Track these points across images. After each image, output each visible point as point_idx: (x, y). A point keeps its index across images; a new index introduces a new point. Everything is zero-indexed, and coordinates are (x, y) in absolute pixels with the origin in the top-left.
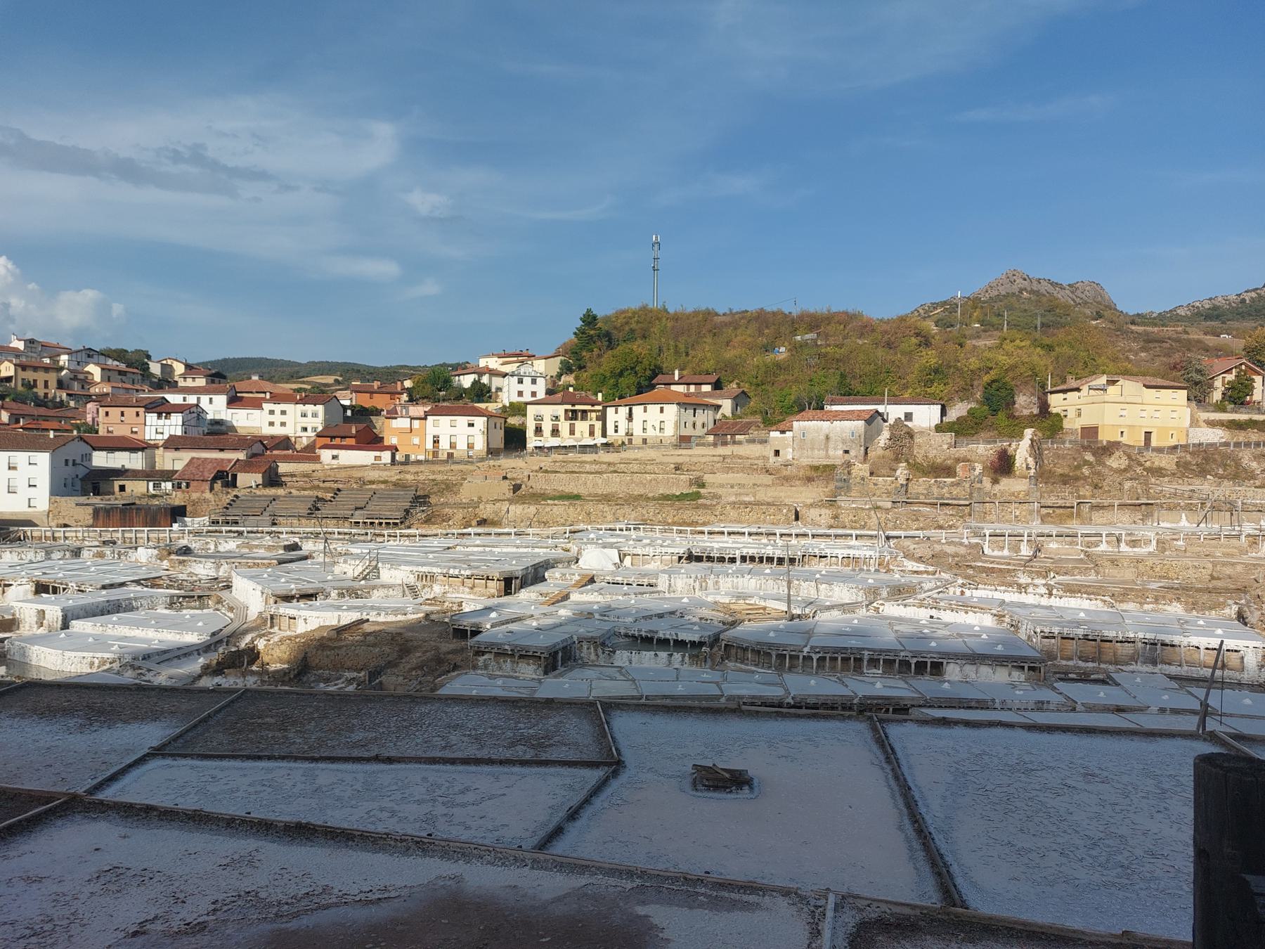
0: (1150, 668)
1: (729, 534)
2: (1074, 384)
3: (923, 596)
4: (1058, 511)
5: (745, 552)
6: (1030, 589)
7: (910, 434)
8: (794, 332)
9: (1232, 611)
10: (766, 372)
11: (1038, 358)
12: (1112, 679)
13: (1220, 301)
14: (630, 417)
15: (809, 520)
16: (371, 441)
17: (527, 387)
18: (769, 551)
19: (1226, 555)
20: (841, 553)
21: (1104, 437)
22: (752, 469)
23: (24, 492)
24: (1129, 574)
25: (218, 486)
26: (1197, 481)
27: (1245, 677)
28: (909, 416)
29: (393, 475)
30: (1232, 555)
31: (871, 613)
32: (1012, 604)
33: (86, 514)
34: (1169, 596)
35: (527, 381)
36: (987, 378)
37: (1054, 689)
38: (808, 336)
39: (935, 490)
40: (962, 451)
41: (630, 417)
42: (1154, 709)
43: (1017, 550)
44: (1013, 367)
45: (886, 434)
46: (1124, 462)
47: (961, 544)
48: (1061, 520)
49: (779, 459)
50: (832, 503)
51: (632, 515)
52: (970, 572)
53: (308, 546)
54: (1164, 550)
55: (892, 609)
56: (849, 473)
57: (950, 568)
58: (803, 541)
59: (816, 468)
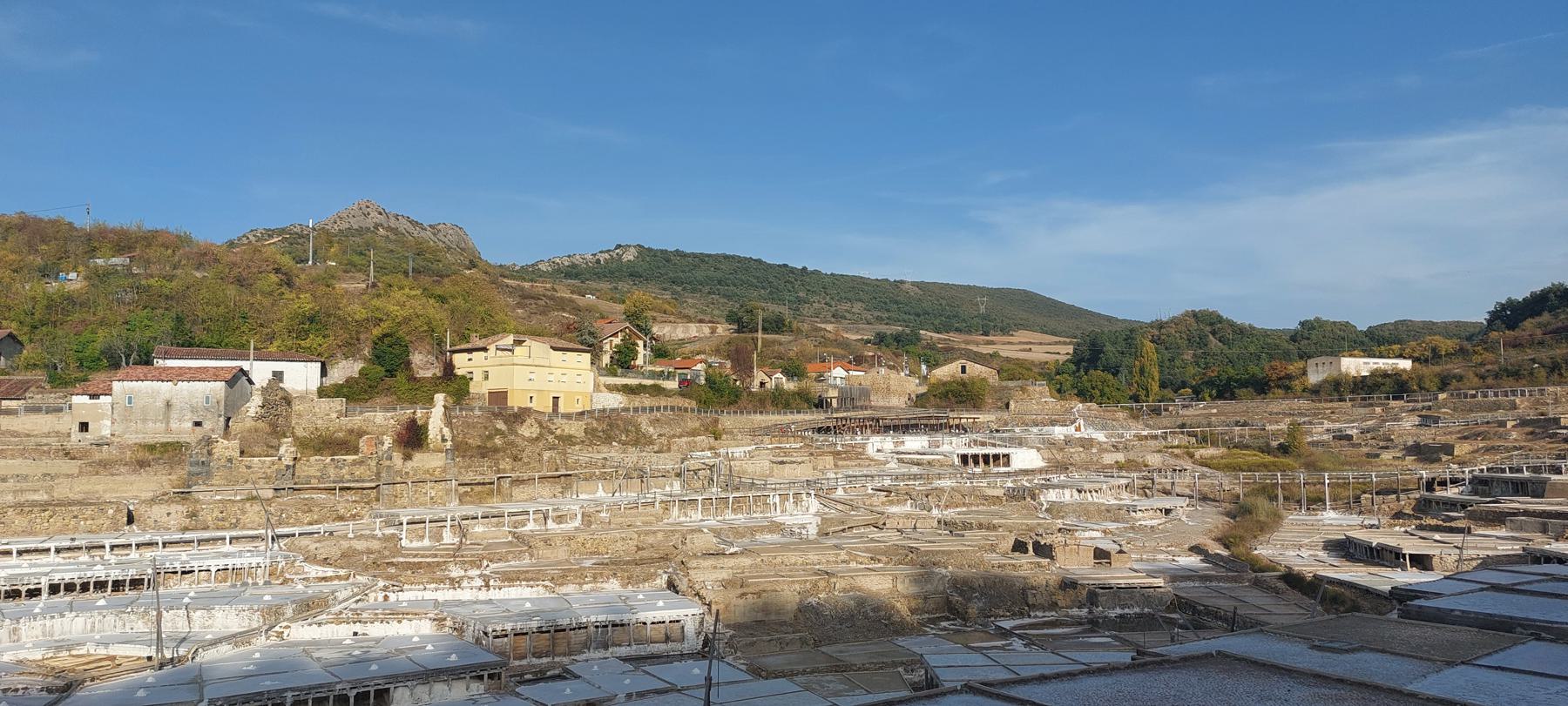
0: (600, 654)
1: (20, 553)
2: (480, 344)
3: (338, 608)
4: (479, 488)
5: (56, 578)
6: (465, 584)
7: (287, 400)
8: (92, 252)
9: (662, 581)
10: (48, 307)
11: (433, 310)
12: (568, 671)
13: (577, 260)
15: (150, 522)
18: (99, 572)
19: (645, 523)
20: (214, 564)
21: (515, 402)
22: (40, 451)
24: (561, 554)
26: (605, 448)
27: (685, 648)
28: (278, 376)
30: (651, 524)
31: (274, 640)
32: (447, 603)
34: (606, 572)
36: (377, 332)
37: (518, 695)
38: (115, 260)
39: (332, 472)
42: (622, 696)
43: (439, 538)
44: (407, 320)
45: (257, 400)
46: (535, 431)
47: (374, 537)
48: (480, 499)
49: (88, 436)
50: (184, 495)
52: (392, 570)
54: (590, 523)
55: (301, 632)
56: (210, 453)
57: (366, 568)
58: (148, 554)
59: (151, 448)
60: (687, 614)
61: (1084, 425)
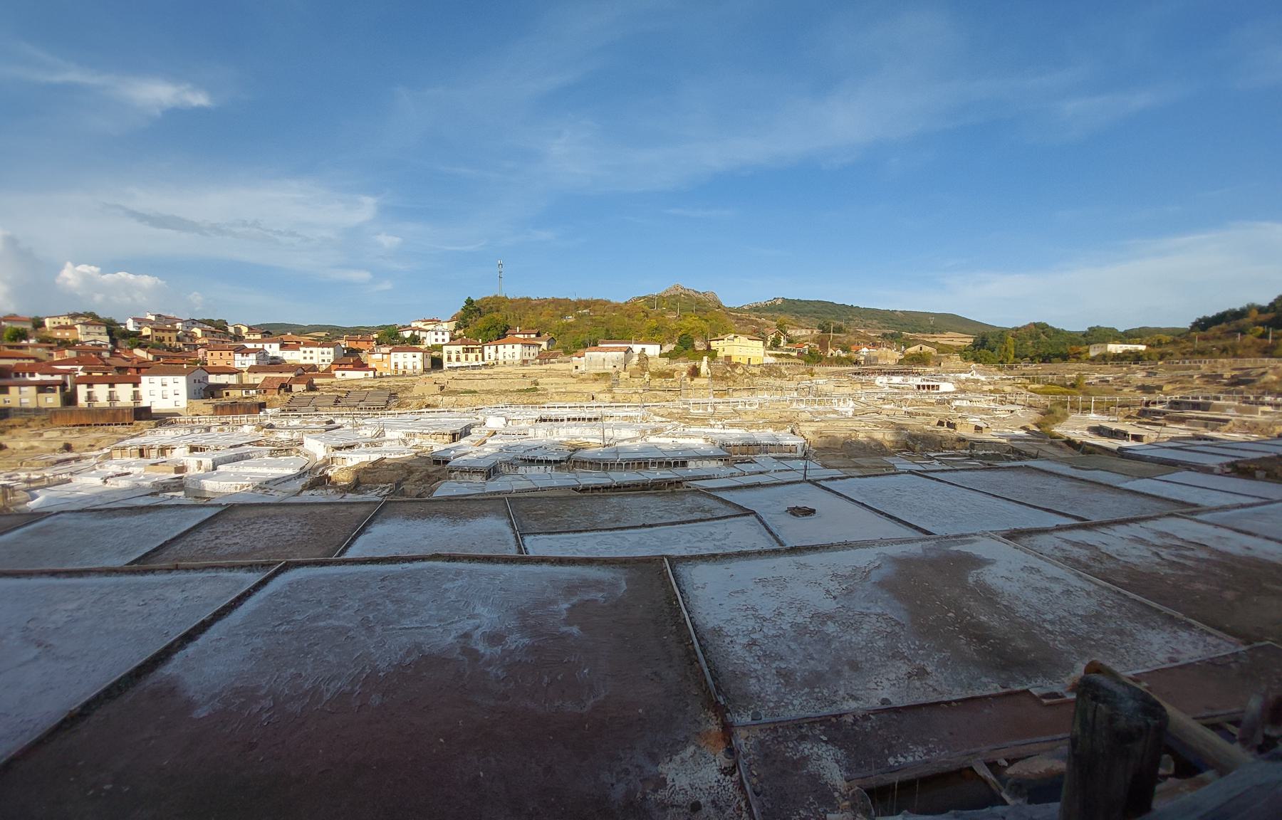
16: (361, 366)
23: (172, 398)
25: (282, 391)
29: (376, 383)
33: (209, 409)
40: (673, 366)
51: (505, 400)
53: (338, 422)
60: (796, 441)
61: (975, 373)
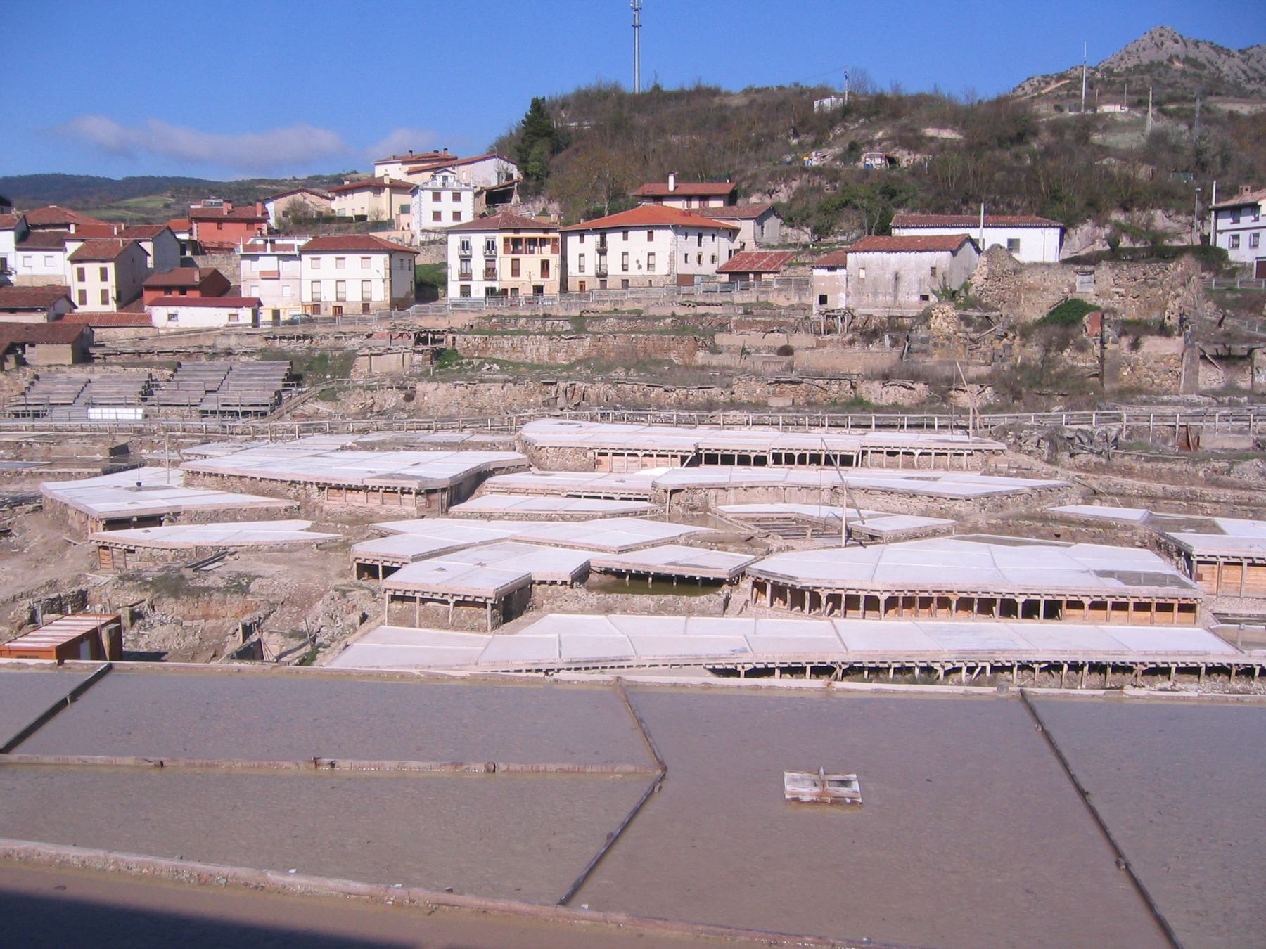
14: (602, 251)
16: (217, 290)
17: (447, 205)
35: (447, 196)
41: (602, 251)
